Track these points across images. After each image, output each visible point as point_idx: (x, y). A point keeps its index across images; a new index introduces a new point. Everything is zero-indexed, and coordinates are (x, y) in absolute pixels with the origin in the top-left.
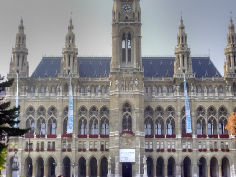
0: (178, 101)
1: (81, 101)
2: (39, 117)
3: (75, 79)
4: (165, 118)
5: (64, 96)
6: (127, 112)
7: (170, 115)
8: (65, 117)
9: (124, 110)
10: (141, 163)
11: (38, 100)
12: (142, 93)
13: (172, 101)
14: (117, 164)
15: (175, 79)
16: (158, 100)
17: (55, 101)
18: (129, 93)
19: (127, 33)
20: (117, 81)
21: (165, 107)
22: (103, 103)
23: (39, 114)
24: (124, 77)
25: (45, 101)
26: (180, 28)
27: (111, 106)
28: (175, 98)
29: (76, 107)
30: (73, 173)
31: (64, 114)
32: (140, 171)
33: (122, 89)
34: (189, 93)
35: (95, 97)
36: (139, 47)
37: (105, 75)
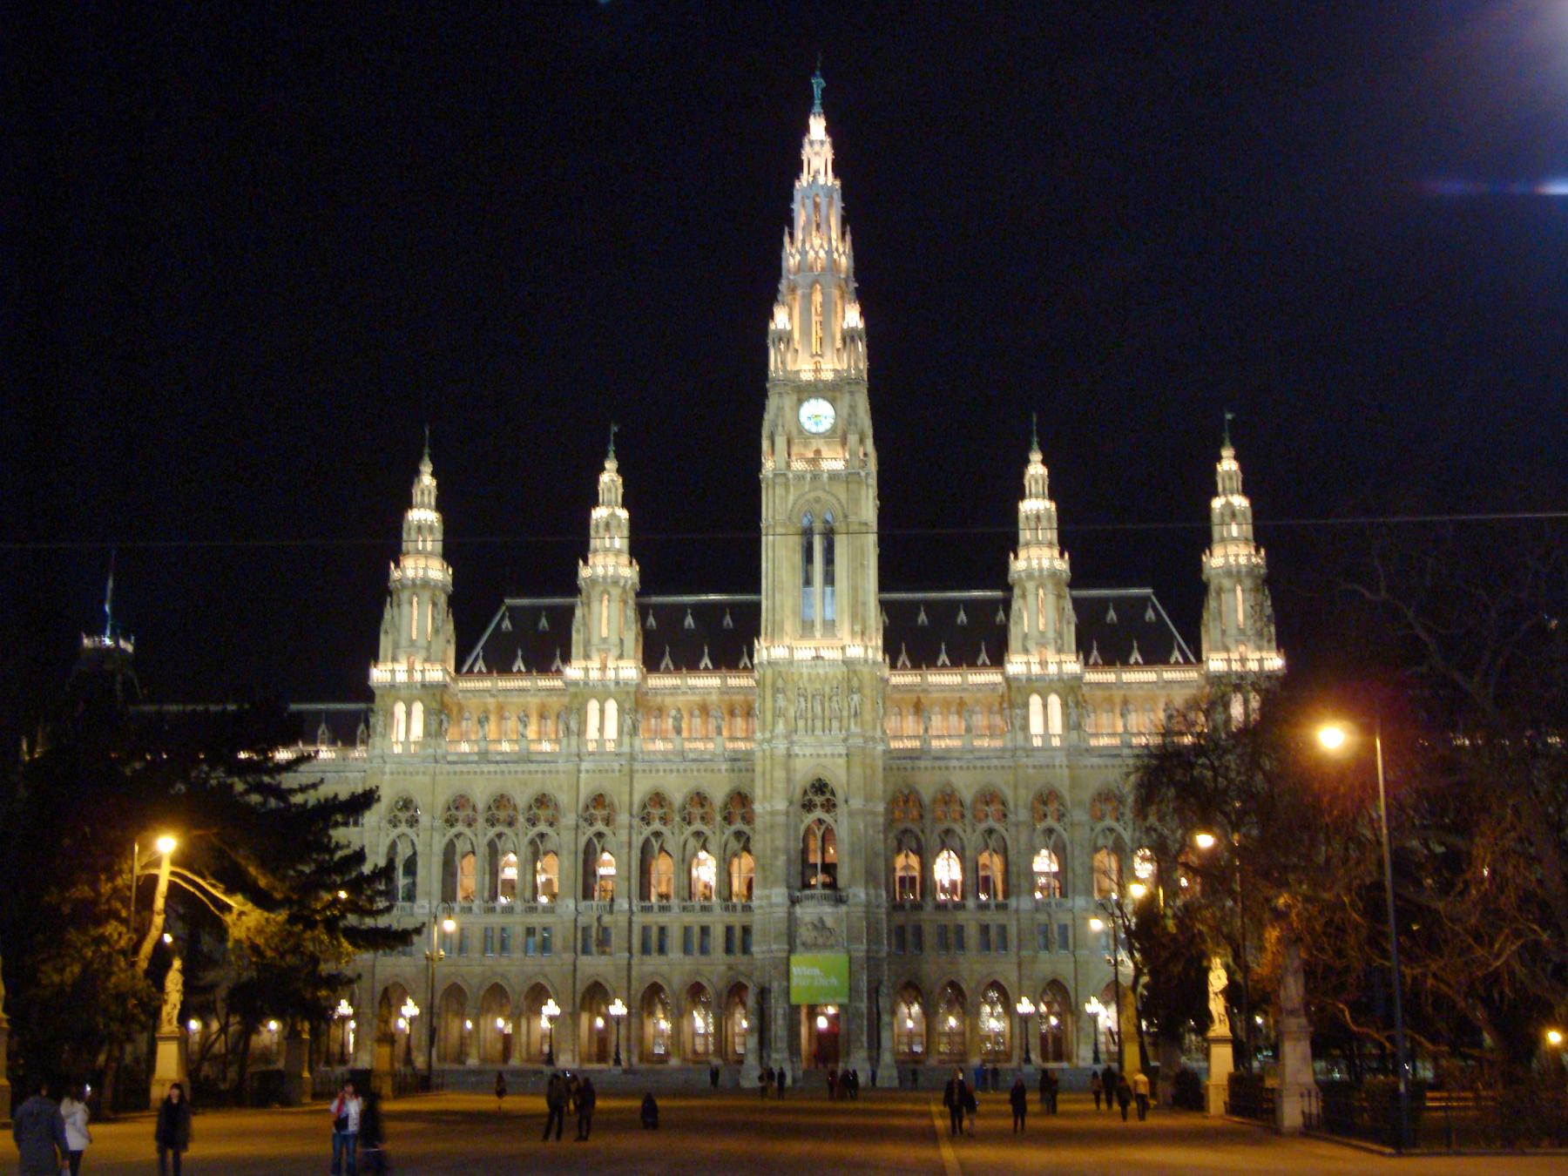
2: (492, 832)
4: (969, 830)
6: (818, 813)
7: (991, 823)
9: (808, 806)
10: (870, 1009)
12: (873, 739)
14: (780, 1011)
15: (1007, 680)
16: (942, 763)
18: (825, 739)
20: (780, 696)
21: (966, 785)
23: (492, 822)
24: (805, 677)
27: (758, 792)
29: (631, 795)
30: (618, 1045)
32: (865, 1038)
33: (801, 723)
36: (862, 565)
37: (745, 668)
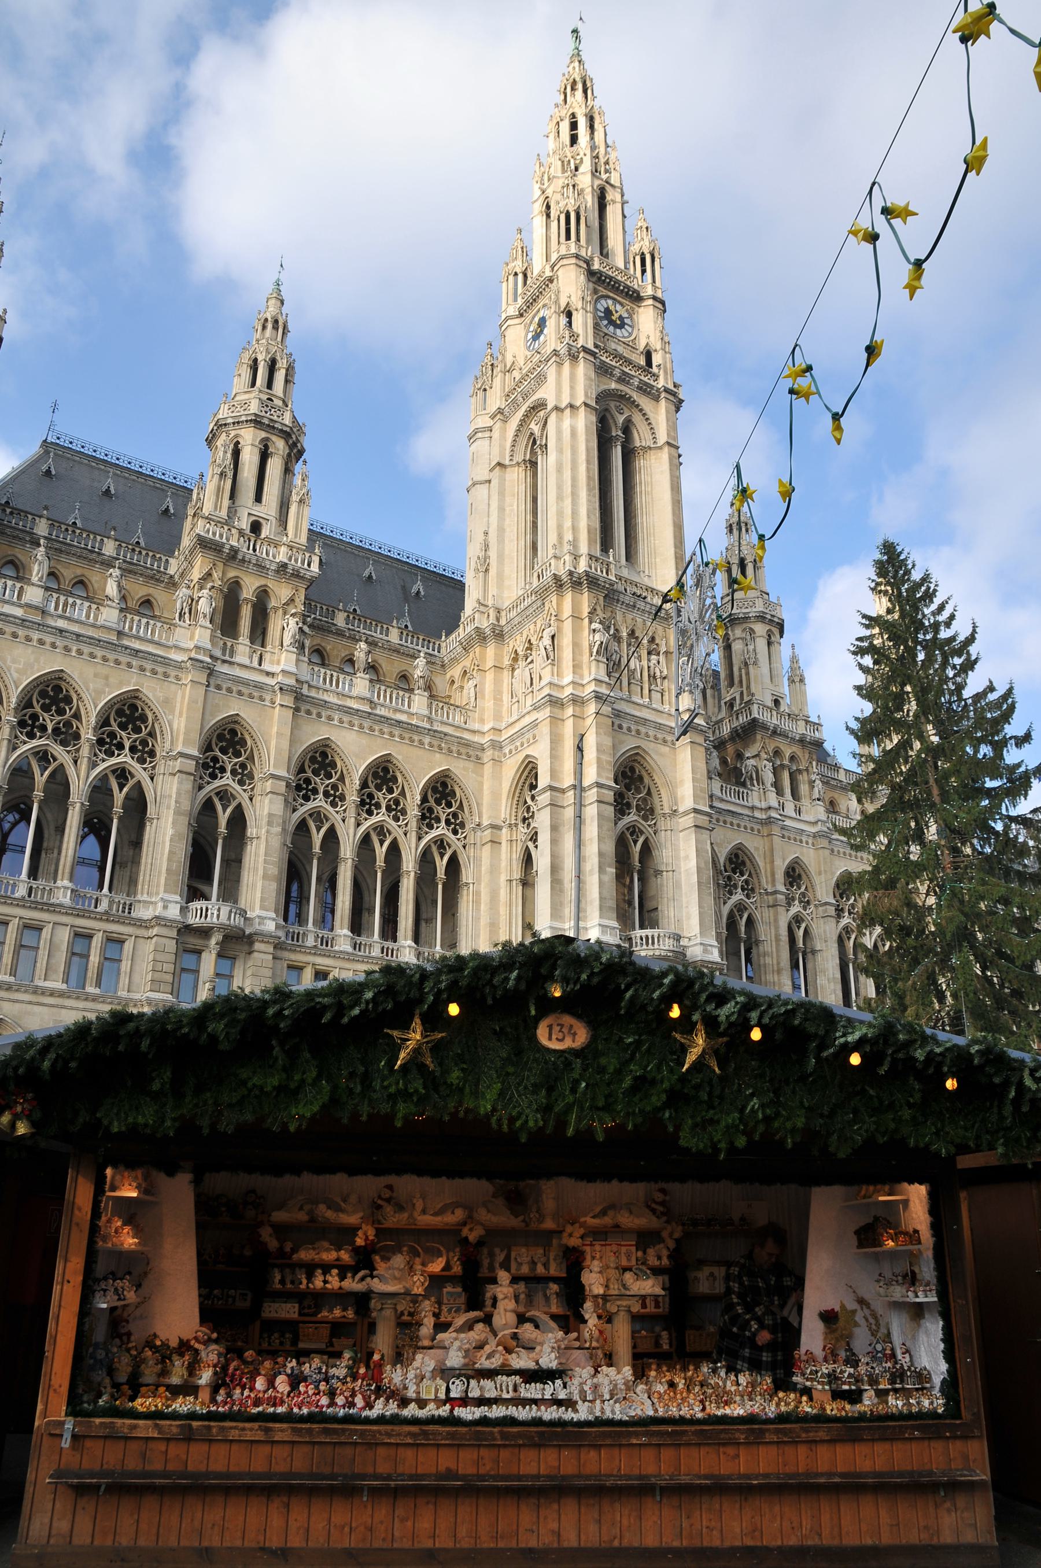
0: (776, 830)
1: (319, 715)
3: (297, 575)
5: (218, 653)
8: (208, 788)
11: (36, 636)
13: (745, 827)
17: (154, 672)
19: (621, 419)
22: (438, 755)
25: (86, 650)
26: (730, 529)
28: (757, 814)
31: (205, 766)
34: (805, 802)
35: (396, 710)
